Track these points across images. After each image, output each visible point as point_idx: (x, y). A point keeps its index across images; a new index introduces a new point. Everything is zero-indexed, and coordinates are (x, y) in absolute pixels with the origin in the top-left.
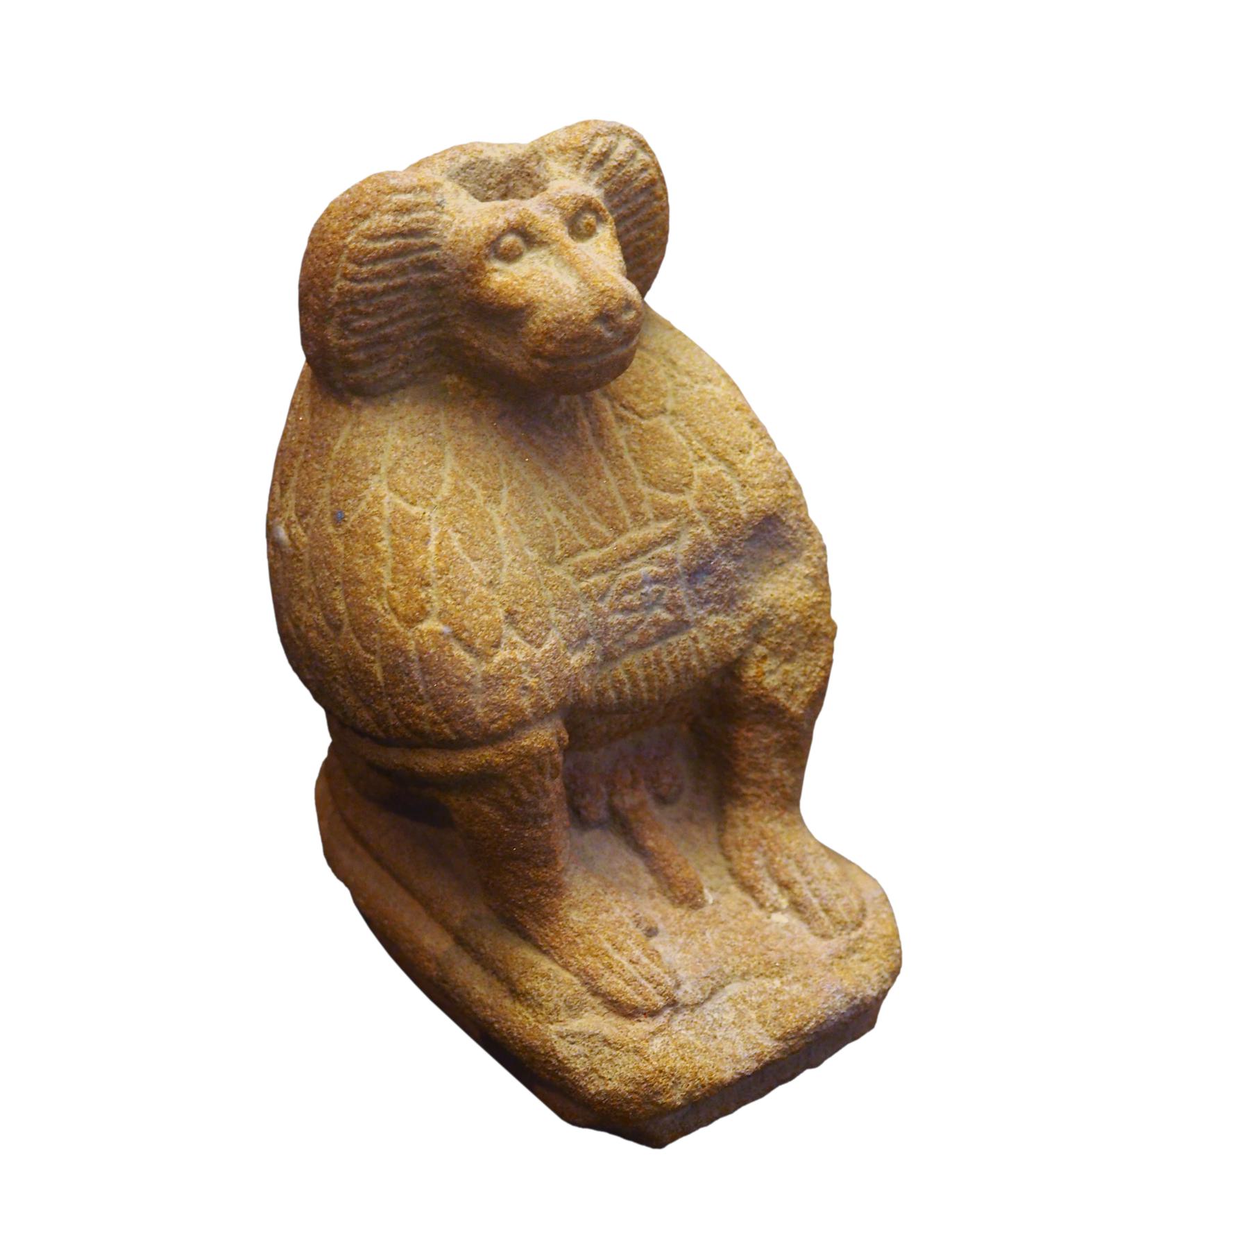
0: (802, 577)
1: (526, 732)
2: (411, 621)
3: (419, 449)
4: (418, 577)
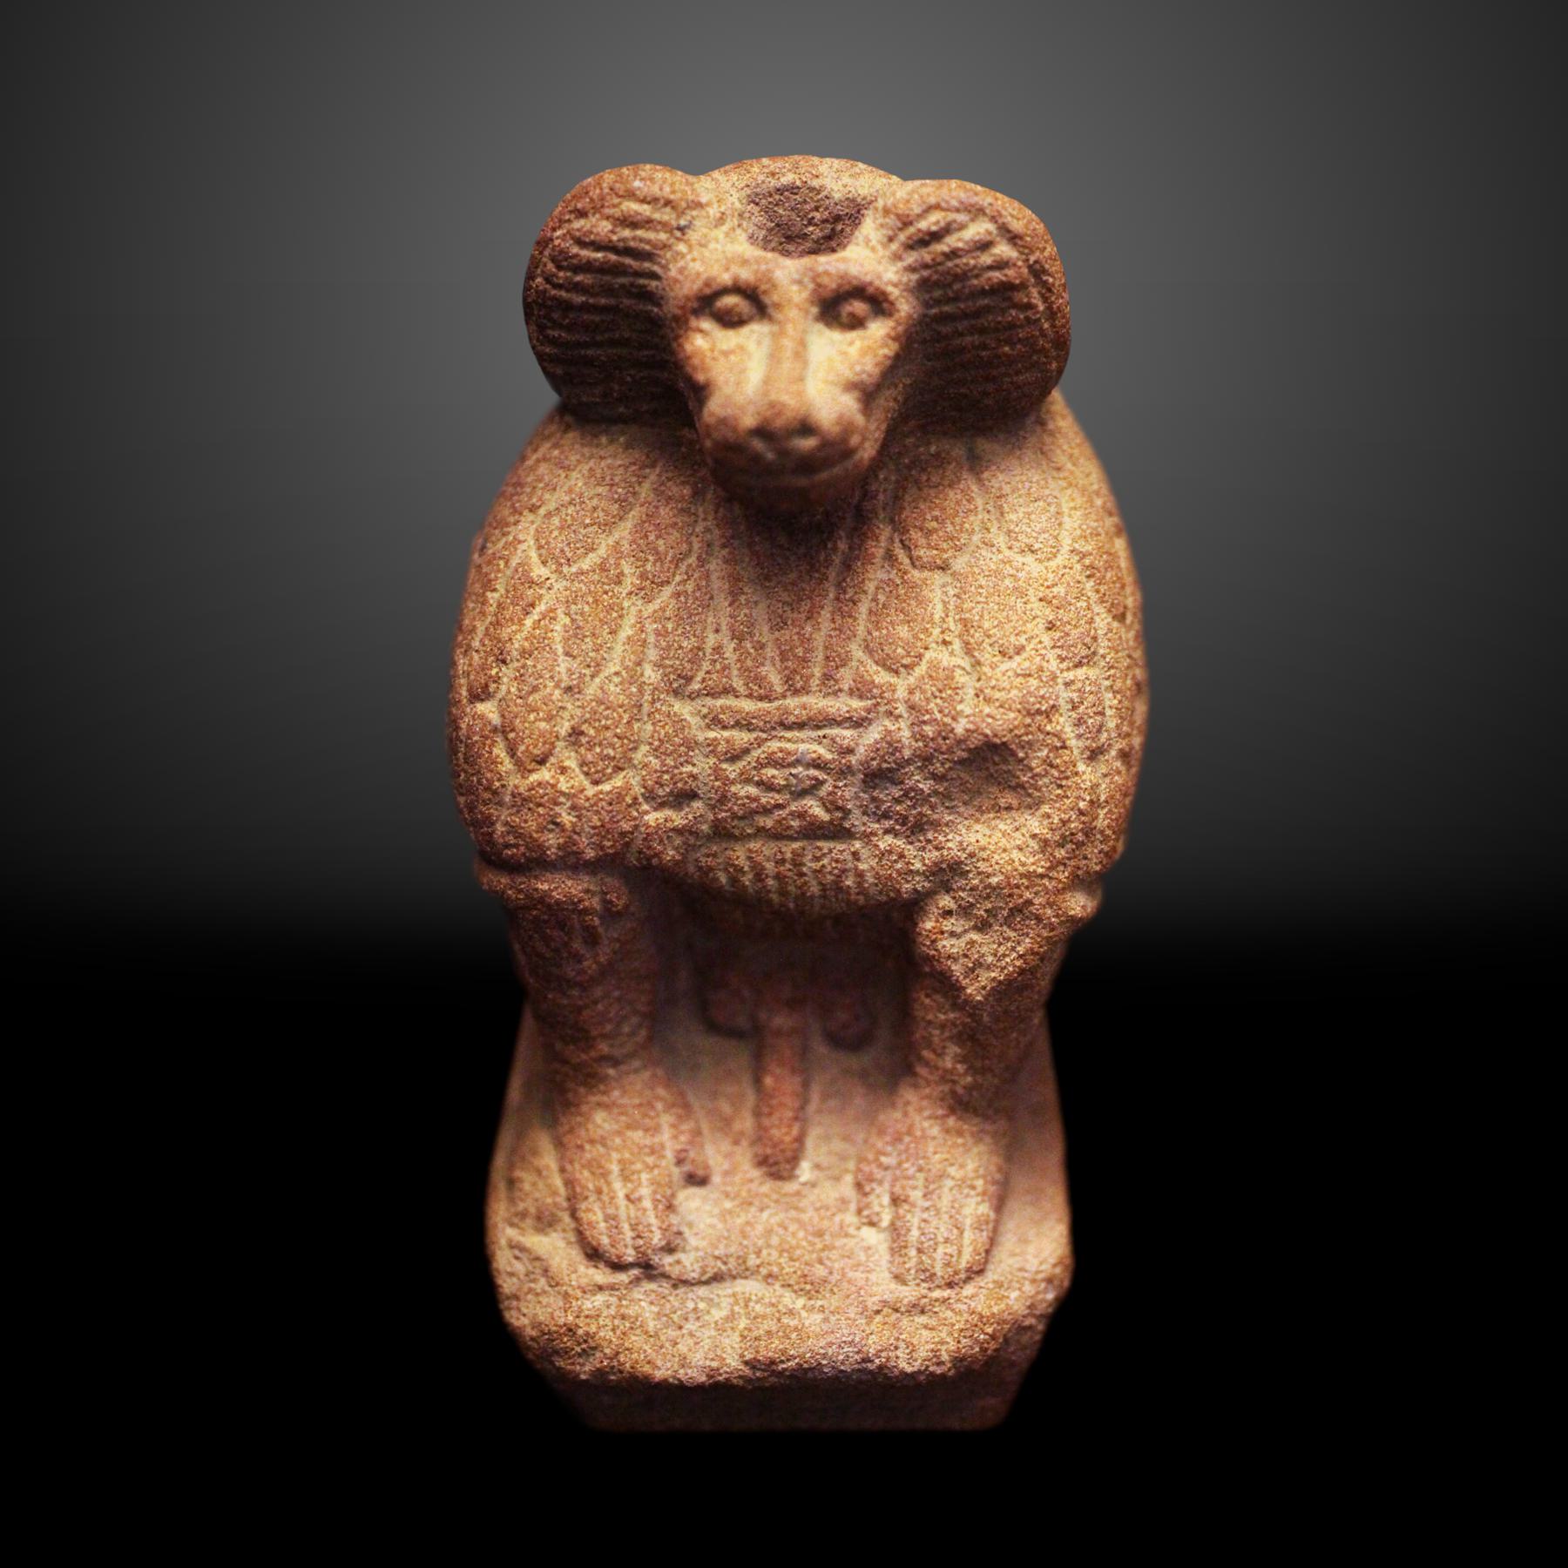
0: (1027, 835)
1: (548, 874)
2: (475, 697)
3: (595, 502)
4: (499, 649)
